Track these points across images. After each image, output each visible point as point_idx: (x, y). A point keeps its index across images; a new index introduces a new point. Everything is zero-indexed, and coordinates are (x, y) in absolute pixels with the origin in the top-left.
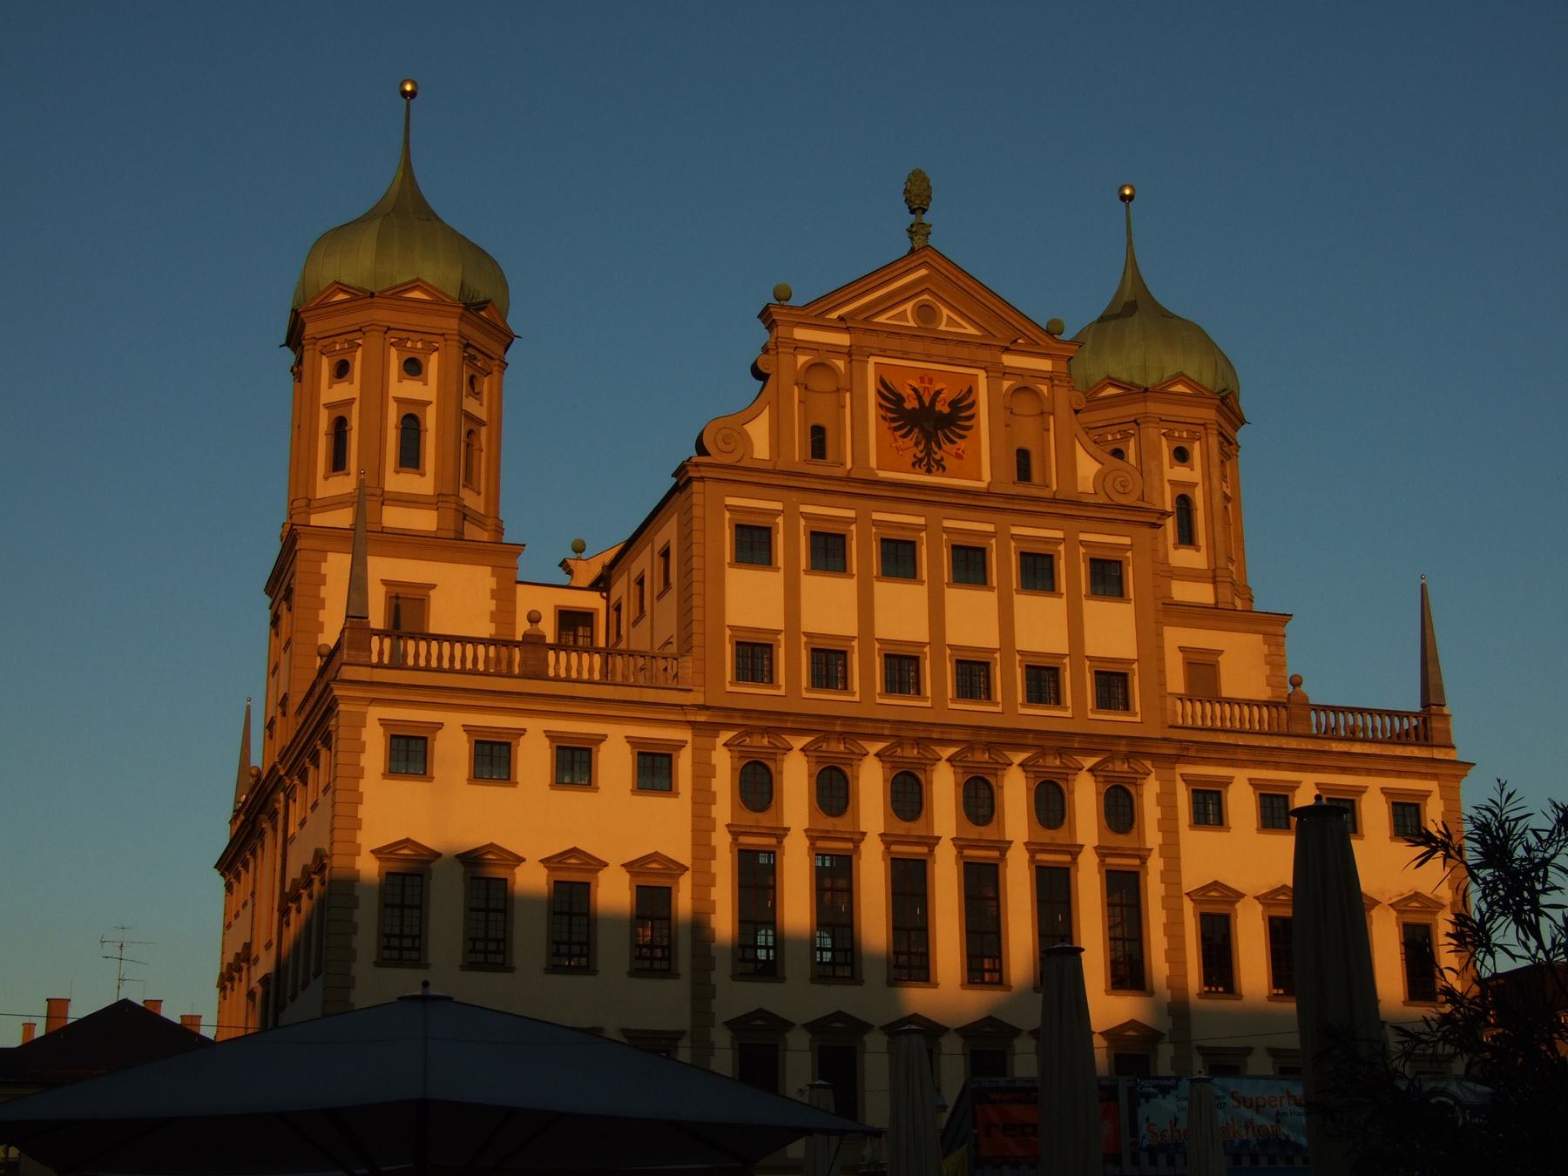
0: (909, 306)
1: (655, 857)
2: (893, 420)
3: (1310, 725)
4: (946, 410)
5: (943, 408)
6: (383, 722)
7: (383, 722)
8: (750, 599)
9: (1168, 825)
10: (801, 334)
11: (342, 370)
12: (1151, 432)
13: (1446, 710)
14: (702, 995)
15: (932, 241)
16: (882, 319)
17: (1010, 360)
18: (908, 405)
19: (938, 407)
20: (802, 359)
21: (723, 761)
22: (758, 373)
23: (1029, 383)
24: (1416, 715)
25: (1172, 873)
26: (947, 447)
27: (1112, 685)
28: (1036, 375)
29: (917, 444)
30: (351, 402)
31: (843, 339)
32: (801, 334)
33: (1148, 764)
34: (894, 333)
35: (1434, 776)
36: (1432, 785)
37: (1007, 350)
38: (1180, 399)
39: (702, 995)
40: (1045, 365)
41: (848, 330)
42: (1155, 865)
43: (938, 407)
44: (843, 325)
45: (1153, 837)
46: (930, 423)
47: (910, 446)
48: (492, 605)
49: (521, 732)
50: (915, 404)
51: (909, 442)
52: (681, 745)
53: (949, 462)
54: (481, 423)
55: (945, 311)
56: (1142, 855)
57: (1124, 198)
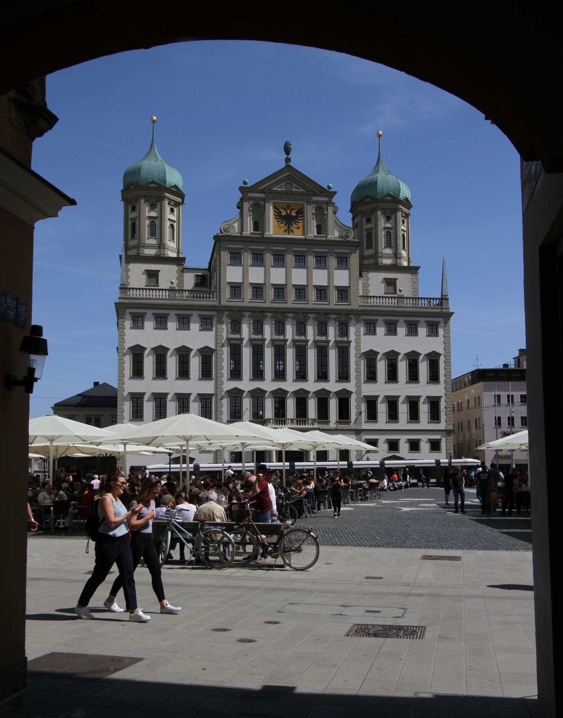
0: (283, 184)
1: (207, 347)
2: (278, 219)
3: (404, 304)
4: (294, 215)
5: (293, 214)
6: (131, 313)
7: (131, 313)
8: (233, 274)
9: (357, 334)
10: (250, 195)
11: (134, 209)
13: (448, 297)
15: (291, 164)
16: (275, 189)
18: (283, 214)
19: (292, 214)
22: (238, 208)
24: (439, 299)
25: (358, 347)
26: (295, 226)
28: (323, 203)
29: (285, 226)
30: (135, 218)
31: (262, 195)
32: (250, 195)
33: (352, 316)
34: (278, 193)
35: (442, 317)
36: (441, 320)
37: (313, 196)
38: (388, 201)
40: (325, 199)
41: (264, 193)
42: (353, 345)
43: (292, 214)
44: (262, 191)
45: (352, 336)
47: (283, 226)
48: (177, 275)
49: (169, 314)
50: (285, 214)
51: (283, 225)
52: (213, 316)
53: (295, 230)
54: (174, 221)
55: (294, 185)
56: (349, 342)
57: (380, 136)
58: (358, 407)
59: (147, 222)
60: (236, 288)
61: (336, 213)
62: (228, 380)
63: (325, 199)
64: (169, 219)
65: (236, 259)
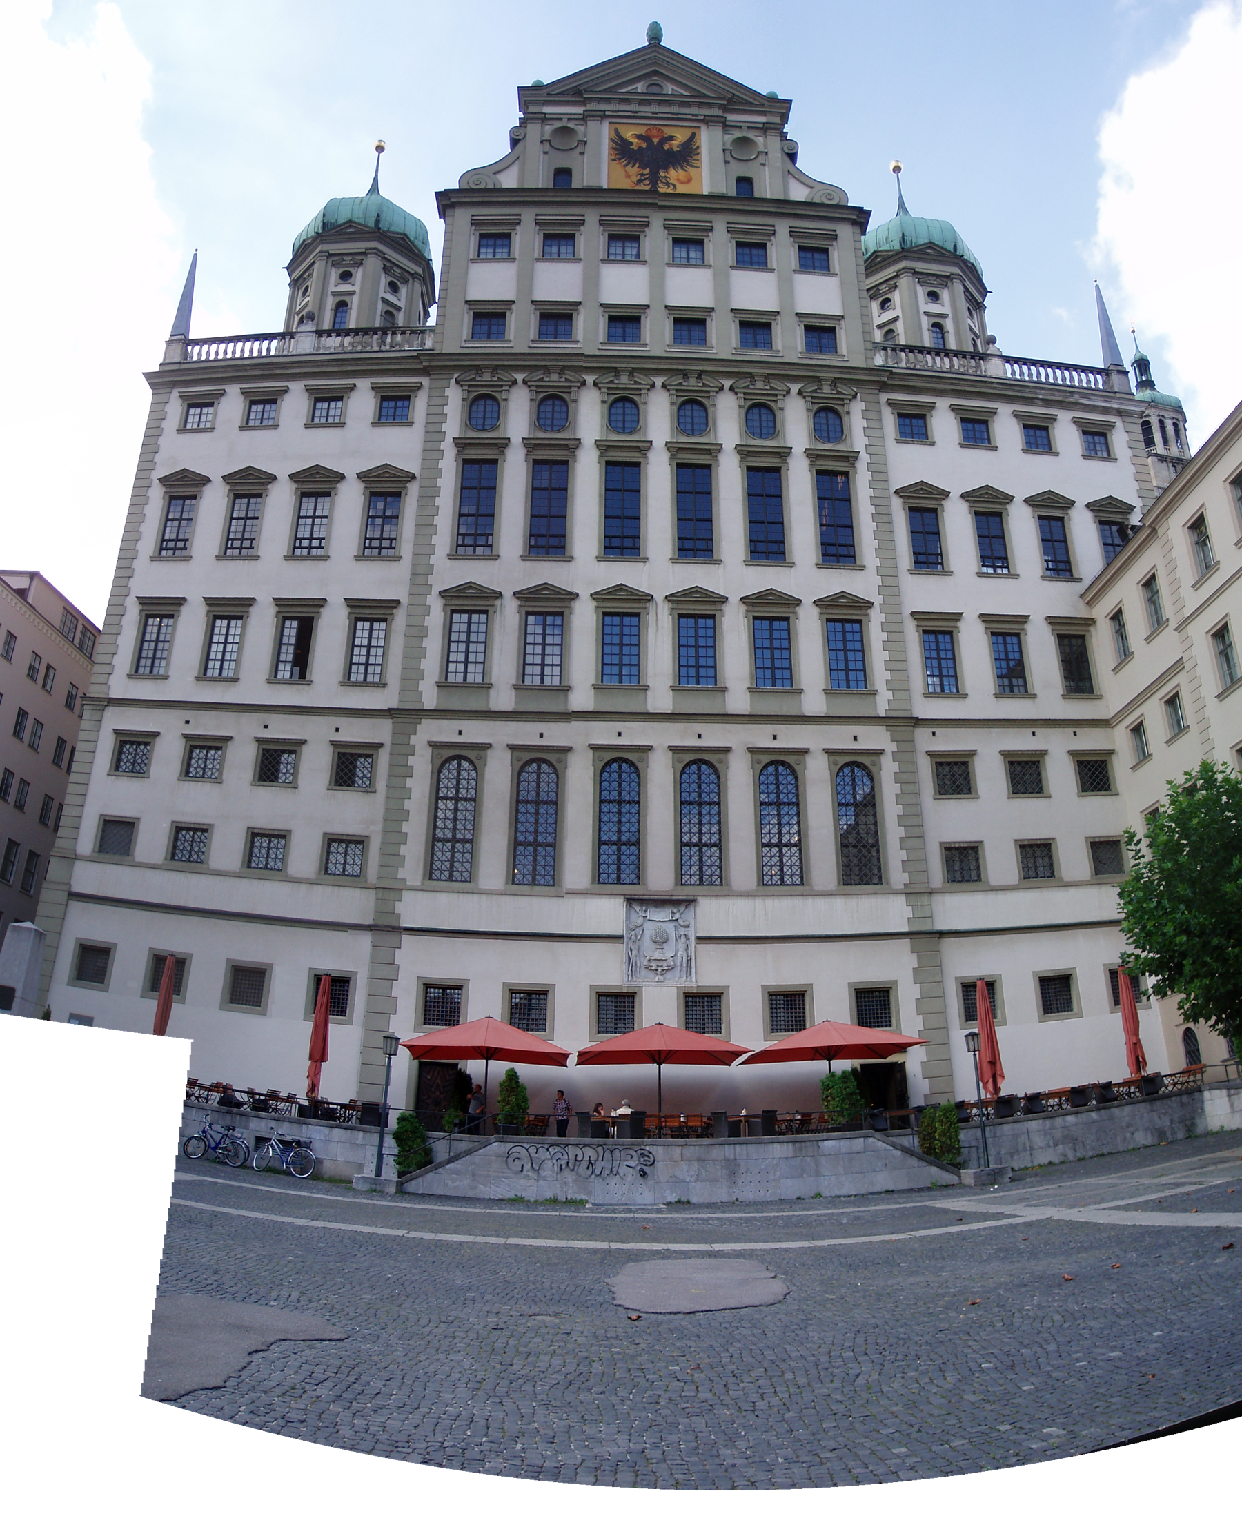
10: (547, 110)
12: (905, 282)
14: (420, 575)
17: (731, 117)
20: (548, 129)
21: (455, 397)
22: (515, 142)
23: (750, 135)
25: (879, 472)
27: (820, 332)
32: (547, 110)
37: (726, 109)
39: (420, 575)
40: (762, 119)
41: (584, 102)
46: (657, 157)
56: (851, 458)
58: (895, 645)
59: (330, 303)
60: (489, 317)
61: (792, 157)
62: (451, 557)
63: (762, 119)
64: (384, 300)
65: (494, 240)
